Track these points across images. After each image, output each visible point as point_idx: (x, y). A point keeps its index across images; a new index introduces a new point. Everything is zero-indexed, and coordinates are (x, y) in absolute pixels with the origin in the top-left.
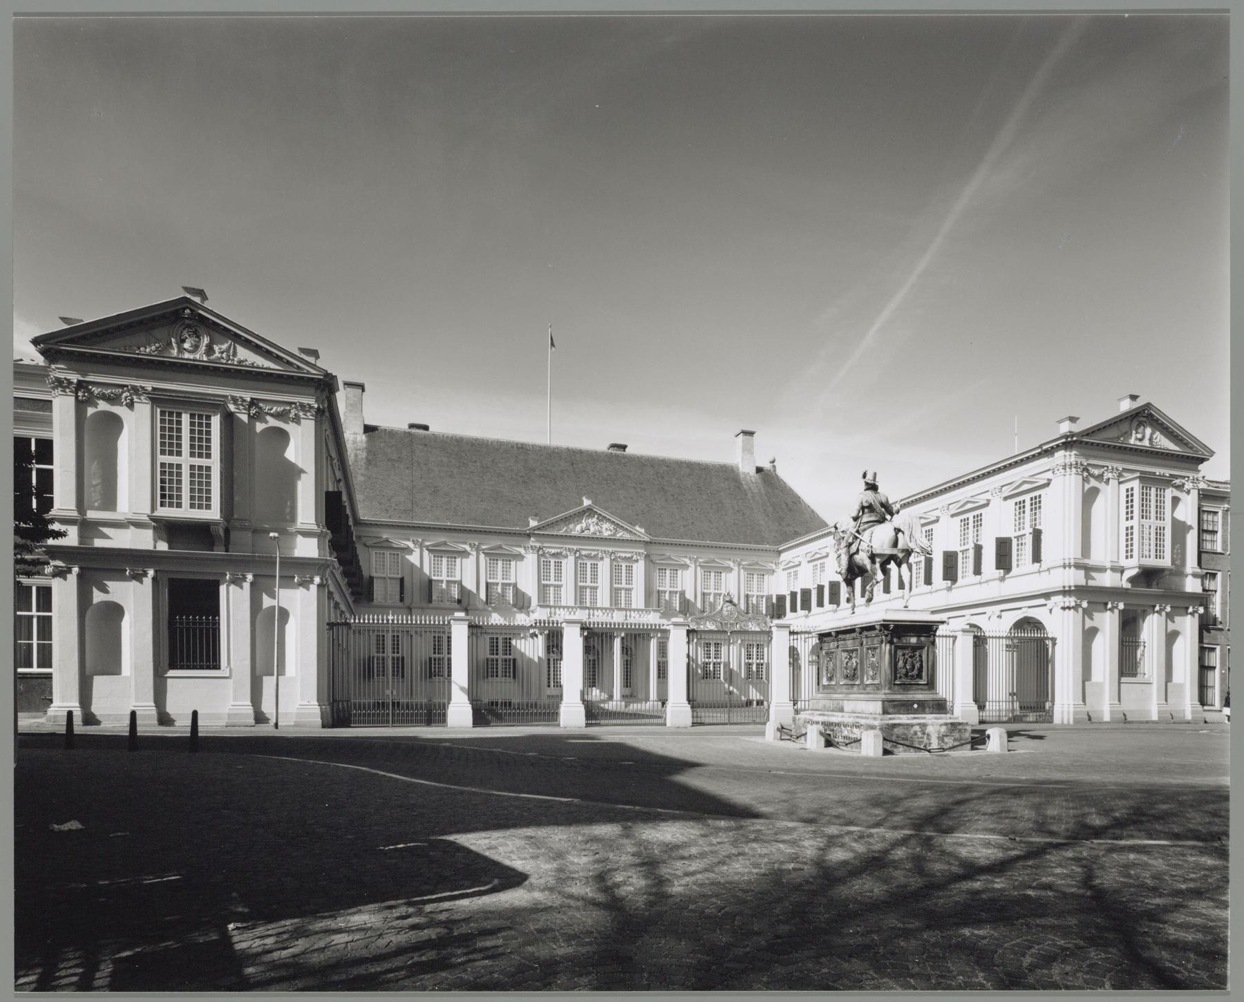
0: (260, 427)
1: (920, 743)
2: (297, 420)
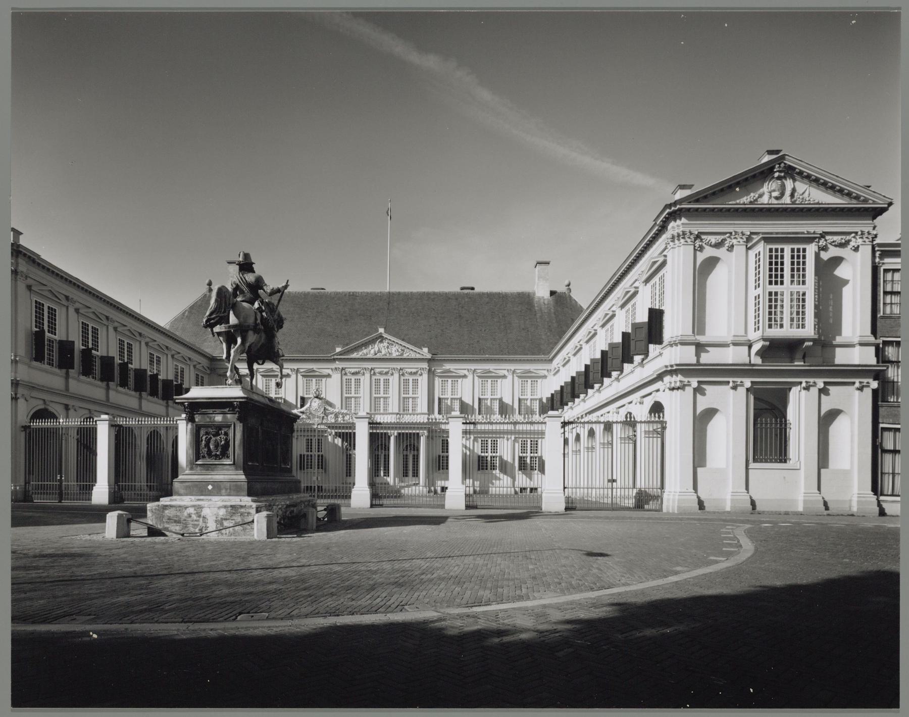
1: (195, 526)
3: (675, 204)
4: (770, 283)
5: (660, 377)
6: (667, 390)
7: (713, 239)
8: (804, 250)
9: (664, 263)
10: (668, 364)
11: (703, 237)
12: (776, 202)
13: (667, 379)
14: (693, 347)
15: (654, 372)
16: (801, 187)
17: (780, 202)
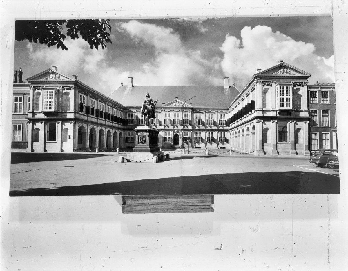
0: (64, 92)
2: (71, 90)
3: (256, 74)
4: (281, 95)
5: (254, 119)
6: (256, 123)
7: (267, 83)
8: (289, 87)
9: (255, 89)
10: (255, 116)
11: (264, 83)
12: (282, 74)
13: (256, 120)
14: (262, 112)
15: (253, 118)
16: (289, 70)
17: (283, 74)
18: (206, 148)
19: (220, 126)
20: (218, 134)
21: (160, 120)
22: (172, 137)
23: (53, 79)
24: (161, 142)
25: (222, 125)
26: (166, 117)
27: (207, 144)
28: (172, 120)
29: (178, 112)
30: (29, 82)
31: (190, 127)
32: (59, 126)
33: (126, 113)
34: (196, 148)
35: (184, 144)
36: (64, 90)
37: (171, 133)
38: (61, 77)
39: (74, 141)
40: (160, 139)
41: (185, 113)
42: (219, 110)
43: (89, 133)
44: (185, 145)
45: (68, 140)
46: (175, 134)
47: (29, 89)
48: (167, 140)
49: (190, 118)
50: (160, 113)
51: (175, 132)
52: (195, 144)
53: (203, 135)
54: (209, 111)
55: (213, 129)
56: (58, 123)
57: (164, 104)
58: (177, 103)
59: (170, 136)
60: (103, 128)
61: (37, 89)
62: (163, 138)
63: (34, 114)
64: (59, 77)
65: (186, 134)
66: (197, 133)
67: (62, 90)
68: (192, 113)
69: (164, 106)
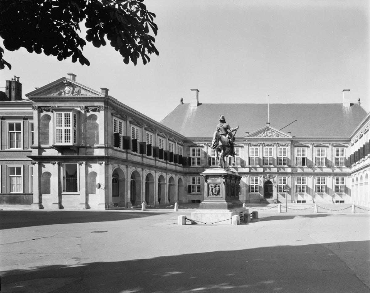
0: (88, 115)
2: (99, 111)
18: (314, 203)
19: (336, 168)
20: (334, 180)
21: (243, 158)
22: (262, 185)
23: (69, 95)
24: (245, 193)
25: (340, 166)
26: (252, 154)
27: (315, 196)
28: (262, 158)
29: (270, 145)
30: (31, 99)
31: (289, 170)
32: (81, 169)
33: (188, 148)
34: (298, 202)
35: (280, 196)
36: (88, 111)
37: (260, 179)
38: (83, 92)
39: (106, 192)
40: (243, 188)
41: (281, 147)
42: (334, 142)
43: (129, 180)
44: (281, 198)
45: (97, 190)
46: (266, 180)
47: (32, 111)
48: (255, 190)
49: (288, 155)
50: (242, 147)
51: (266, 177)
52: (296, 196)
53: (310, 182)
54: (319, 144)
55: (325, 172)
56: (81, 164)
57: (249, 133)
58: (270, 131)
59: (259, 184)
60: (153, 172)
61: (45, 110)
62: (248, 188)
63: (41, 149)
64: (79, 92)
65: (282, 180)
66: (299, 179)
67: (85, 112)
68: (291, 148)
69: (248, 137)
